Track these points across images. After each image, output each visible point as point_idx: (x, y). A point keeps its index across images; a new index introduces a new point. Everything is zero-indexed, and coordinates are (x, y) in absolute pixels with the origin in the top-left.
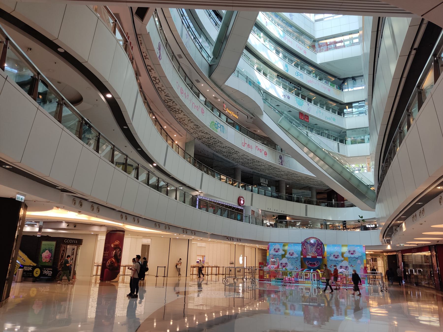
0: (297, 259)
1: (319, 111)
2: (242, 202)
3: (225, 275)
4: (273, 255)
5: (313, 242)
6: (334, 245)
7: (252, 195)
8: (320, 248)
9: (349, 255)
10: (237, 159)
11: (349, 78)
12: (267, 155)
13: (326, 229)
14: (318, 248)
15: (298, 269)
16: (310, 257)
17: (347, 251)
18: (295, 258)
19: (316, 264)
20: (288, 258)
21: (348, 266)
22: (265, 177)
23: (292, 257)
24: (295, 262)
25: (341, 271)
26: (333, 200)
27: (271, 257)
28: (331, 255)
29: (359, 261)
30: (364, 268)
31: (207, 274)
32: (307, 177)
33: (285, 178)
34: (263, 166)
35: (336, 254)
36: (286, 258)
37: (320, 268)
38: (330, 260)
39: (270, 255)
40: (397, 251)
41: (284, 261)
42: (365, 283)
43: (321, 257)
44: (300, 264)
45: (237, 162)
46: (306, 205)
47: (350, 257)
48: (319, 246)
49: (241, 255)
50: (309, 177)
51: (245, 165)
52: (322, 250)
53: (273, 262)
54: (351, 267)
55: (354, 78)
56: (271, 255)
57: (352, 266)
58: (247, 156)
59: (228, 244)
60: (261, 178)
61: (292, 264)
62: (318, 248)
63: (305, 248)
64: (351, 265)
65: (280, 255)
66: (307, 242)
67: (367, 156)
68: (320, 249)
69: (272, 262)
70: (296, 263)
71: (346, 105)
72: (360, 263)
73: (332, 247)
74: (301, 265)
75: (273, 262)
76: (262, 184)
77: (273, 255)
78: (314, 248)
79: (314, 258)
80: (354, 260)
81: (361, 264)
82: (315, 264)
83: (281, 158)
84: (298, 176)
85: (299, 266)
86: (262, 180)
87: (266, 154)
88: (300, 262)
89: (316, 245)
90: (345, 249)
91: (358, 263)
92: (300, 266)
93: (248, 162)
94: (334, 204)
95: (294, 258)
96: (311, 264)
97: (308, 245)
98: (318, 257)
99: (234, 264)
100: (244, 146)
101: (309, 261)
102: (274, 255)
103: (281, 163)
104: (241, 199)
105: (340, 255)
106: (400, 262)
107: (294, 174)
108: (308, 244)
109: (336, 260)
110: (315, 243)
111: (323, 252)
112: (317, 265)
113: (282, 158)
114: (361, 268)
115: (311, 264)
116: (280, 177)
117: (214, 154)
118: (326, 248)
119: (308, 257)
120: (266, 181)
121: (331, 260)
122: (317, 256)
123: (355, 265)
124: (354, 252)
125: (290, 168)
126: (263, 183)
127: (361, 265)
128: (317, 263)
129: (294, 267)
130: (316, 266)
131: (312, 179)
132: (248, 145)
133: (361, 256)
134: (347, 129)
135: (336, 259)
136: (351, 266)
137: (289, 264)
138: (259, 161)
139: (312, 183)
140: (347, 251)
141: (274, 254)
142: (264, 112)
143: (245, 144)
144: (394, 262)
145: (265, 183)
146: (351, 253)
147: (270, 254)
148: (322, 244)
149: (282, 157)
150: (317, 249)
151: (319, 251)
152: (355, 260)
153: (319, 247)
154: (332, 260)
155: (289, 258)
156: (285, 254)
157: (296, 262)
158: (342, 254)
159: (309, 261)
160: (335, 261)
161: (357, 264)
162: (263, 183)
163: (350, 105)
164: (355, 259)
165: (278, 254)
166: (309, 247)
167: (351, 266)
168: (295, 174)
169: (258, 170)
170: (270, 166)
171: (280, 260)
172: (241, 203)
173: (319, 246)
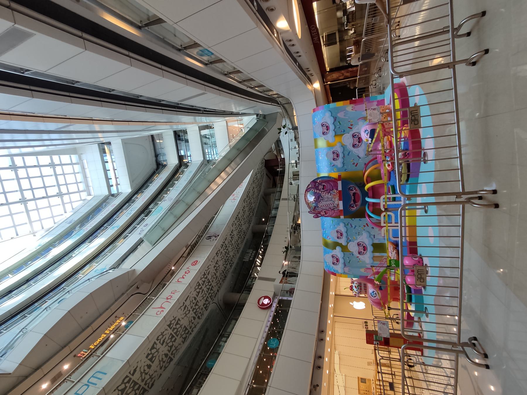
0: (348, 225)
1: (176, 188)
2: (266, 301)
3: (392, 362)
4: (344, 267)
5: (314, 197)
6: (317, 161)
7: (261, 278)
8: (321, 185)
9: (331, 133)
10: (195, 313)
11: (156, 160)
12: (197, 261)
13: (299, 175)
14: (323, 189)
15: (367, 224)
16: (341, 203)
17: (323, 138)
18: (346, 227)
19: (353, 192)
20: (348, 241)
21: (351, 133)
22: (244, 253)
23: (345, 234)
24: (355, 228)
25: (367, 134)
26: (278, 170)
27: (349, 271)
28: (334, 165)
29: (340, 115)
30: (352, 105)
31: (392, 374)
32: (244, 201)
33: (248, 226)
34: (216, 263)
35: (332, 156)
36: (348, 243)
37: (361, 184)
38: (343, 167)
39: (344, 272)
40: (324, 83)
41: (353, 247)
42: (382, 98)
43: (340, 183)
44: (357, 219)
45: (205, 308)
46: (282, 200)
47: (334, 132)
48: (319, 186)
49: (351, 303)
50: (244, 198)
51: (216, 291)
52: (325, 182)
53: (361, 289)
54: (353, 129)
55: (157, 156)
56: (346, 271)
57: (350, 127)
58: (186, 301)
59: (334, 322)
60: (244, 260)
61: (359, 234)
62: (323, 189)
63: (325, 212)
64: (349, 127)
65: (344, 254)
66: (315, 207)
67: (229, 138)
68: (324, 184)
69: (361, 292)
70: (356, 226)
71: (182, 162)
72: (344, 113)
73: (319, 165)
74: (358, 219)
75: (361, 289)
76: (251, 259)
77: (344, 267)
78: (323, 194)
79: (343, 196)
80: (340, 124)
81: (345, 110)
82: (354, 194)
83: (210, 237)
84: (241, 211)
85: (361, 222)
86: (246, 259)
87: (196, 262)
88: (353, 219)
89: (318, 191)
90: (322, 143)
91: (344, 116)
92: (360, 220)
93: (205, 289)
94: (281, 169)
95: (347, 230)
96: (355, 201)
97: (320, 205)
98: (340, 188)
99: (368, 321)
100: (163, 311)
101: (350, 205)
102: (345, 265)
103: (216, 237)
104: (261, 303)
105: (333, 149)
106: (339, 76)
107: (237, 218)
108: (318, 205)
109: (343, 156)
110: (315, 194)
111: (329, 179)
112: (356, 190)
113: (210, 235)
114: (352, 110)
115: (355, 201)
116: (245, 233)
117: (178, 364)
118: (324, 174)
119: (341, 207)
120: (249, 253)
121: (342, 164)
122: (337, 189)
123: (349, 122)
124: (324, 125)
125: (226, 224)
126: (250, 257)
127: (348, 111)
128: (352, 190)
129: (364, 230)
130: (359, 192)
131: (248, 194)
132: (166, 300)
133: (330, 113)
134: (203, 159)
135: (341, 155)
136: (351, 128)
137: (360, 239)
138: (205, 274)
139: (256, 194)
140: (323, 138)
141: (343, 266)
142: (133, 268)
143: (161, 307)
144: (340, 93)
145: (251, 254)
146: (327, 130)
147: (343, 272)
148: (314, 182)
149: (208, 236)
150: (323, 190)
151: (328, 186)
152: (339, 122)
153: (321, 187)
154: (343, 163)
155: (348, 239)
156: (340, 245)
157: (353, 226)
158: (329, 145)
159: (350, 205)
160: (344, 157)
161: (347, 118)
162: (250, 257)
163: (181, 158)
164: (337, 122)
165: (343, 258)
166: (322, 204)
167: (351, 128)
168: (237, 217)
169: (228, 266)
170: (217, 254)
171: (353, 254)
172: (268, 304)
173: (318, 187)
